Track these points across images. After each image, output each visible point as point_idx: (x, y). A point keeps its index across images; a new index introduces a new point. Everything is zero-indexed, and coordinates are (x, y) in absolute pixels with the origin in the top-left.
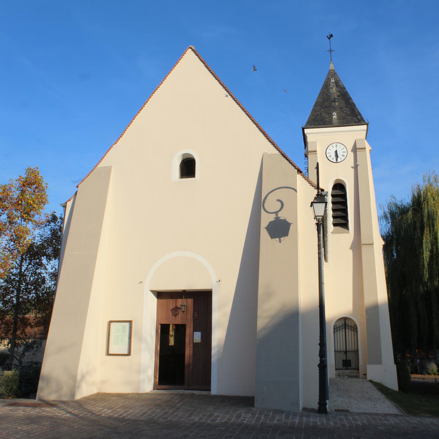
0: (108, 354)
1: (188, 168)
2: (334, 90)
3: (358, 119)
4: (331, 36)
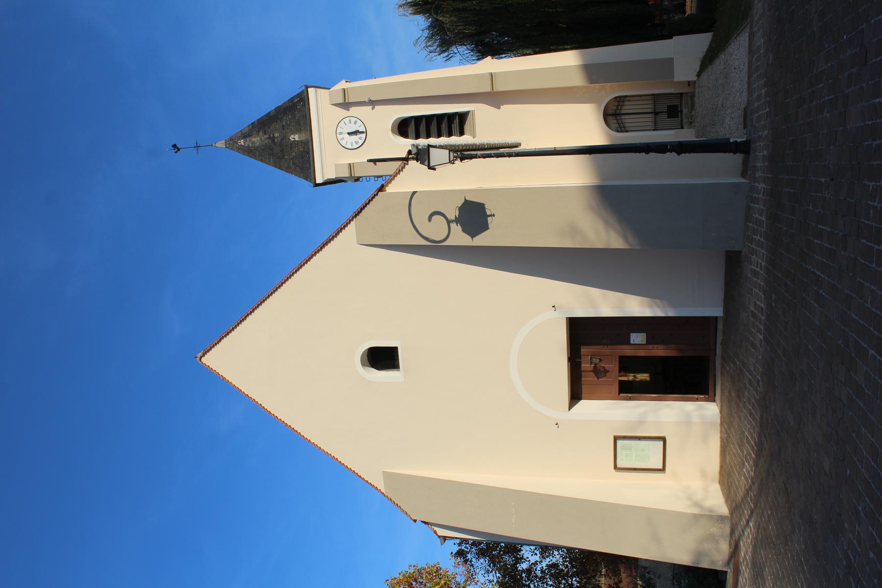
0: (663, 470)
1: (382, 358)
2: (256, 140)
4: (174, 146)
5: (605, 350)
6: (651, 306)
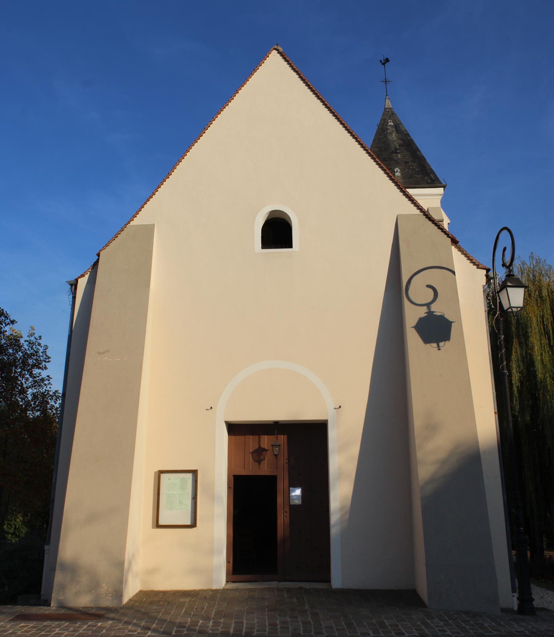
0: (157, 525)
1: (277, 232)
2: (393, 137)
3: (431, 179)
4: (387, 60)
5: (283, 460)
6: (342, 509)
